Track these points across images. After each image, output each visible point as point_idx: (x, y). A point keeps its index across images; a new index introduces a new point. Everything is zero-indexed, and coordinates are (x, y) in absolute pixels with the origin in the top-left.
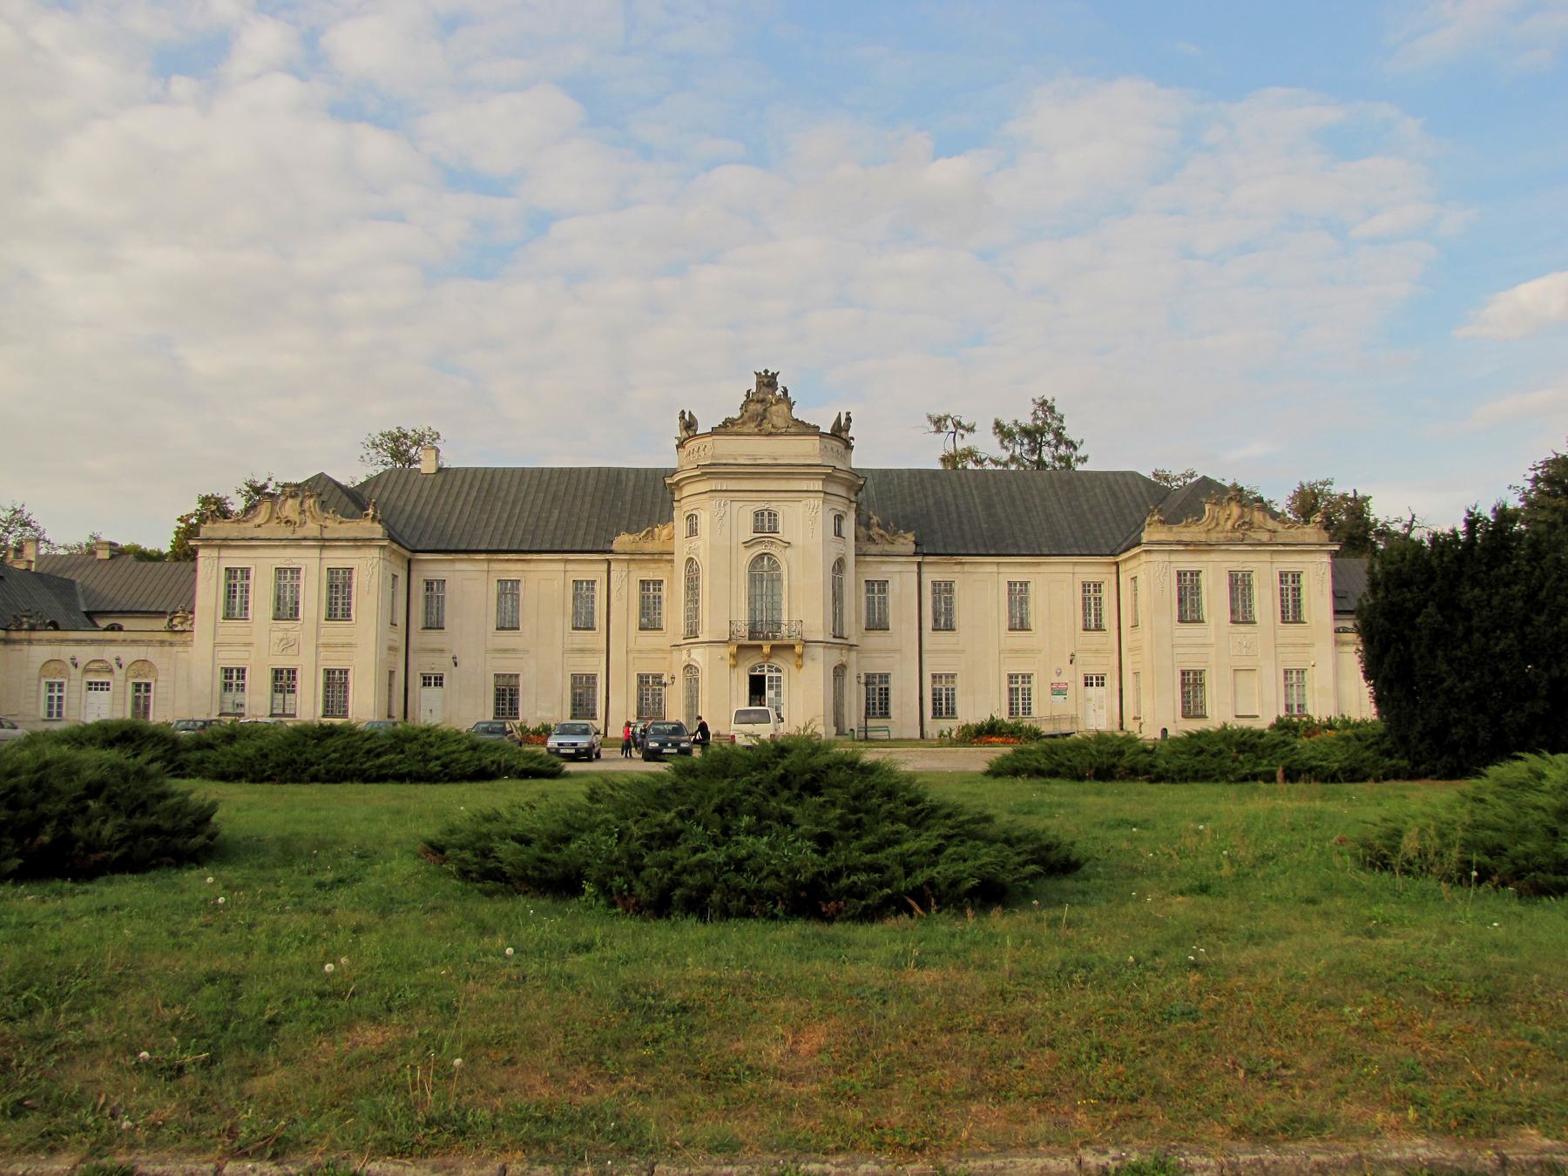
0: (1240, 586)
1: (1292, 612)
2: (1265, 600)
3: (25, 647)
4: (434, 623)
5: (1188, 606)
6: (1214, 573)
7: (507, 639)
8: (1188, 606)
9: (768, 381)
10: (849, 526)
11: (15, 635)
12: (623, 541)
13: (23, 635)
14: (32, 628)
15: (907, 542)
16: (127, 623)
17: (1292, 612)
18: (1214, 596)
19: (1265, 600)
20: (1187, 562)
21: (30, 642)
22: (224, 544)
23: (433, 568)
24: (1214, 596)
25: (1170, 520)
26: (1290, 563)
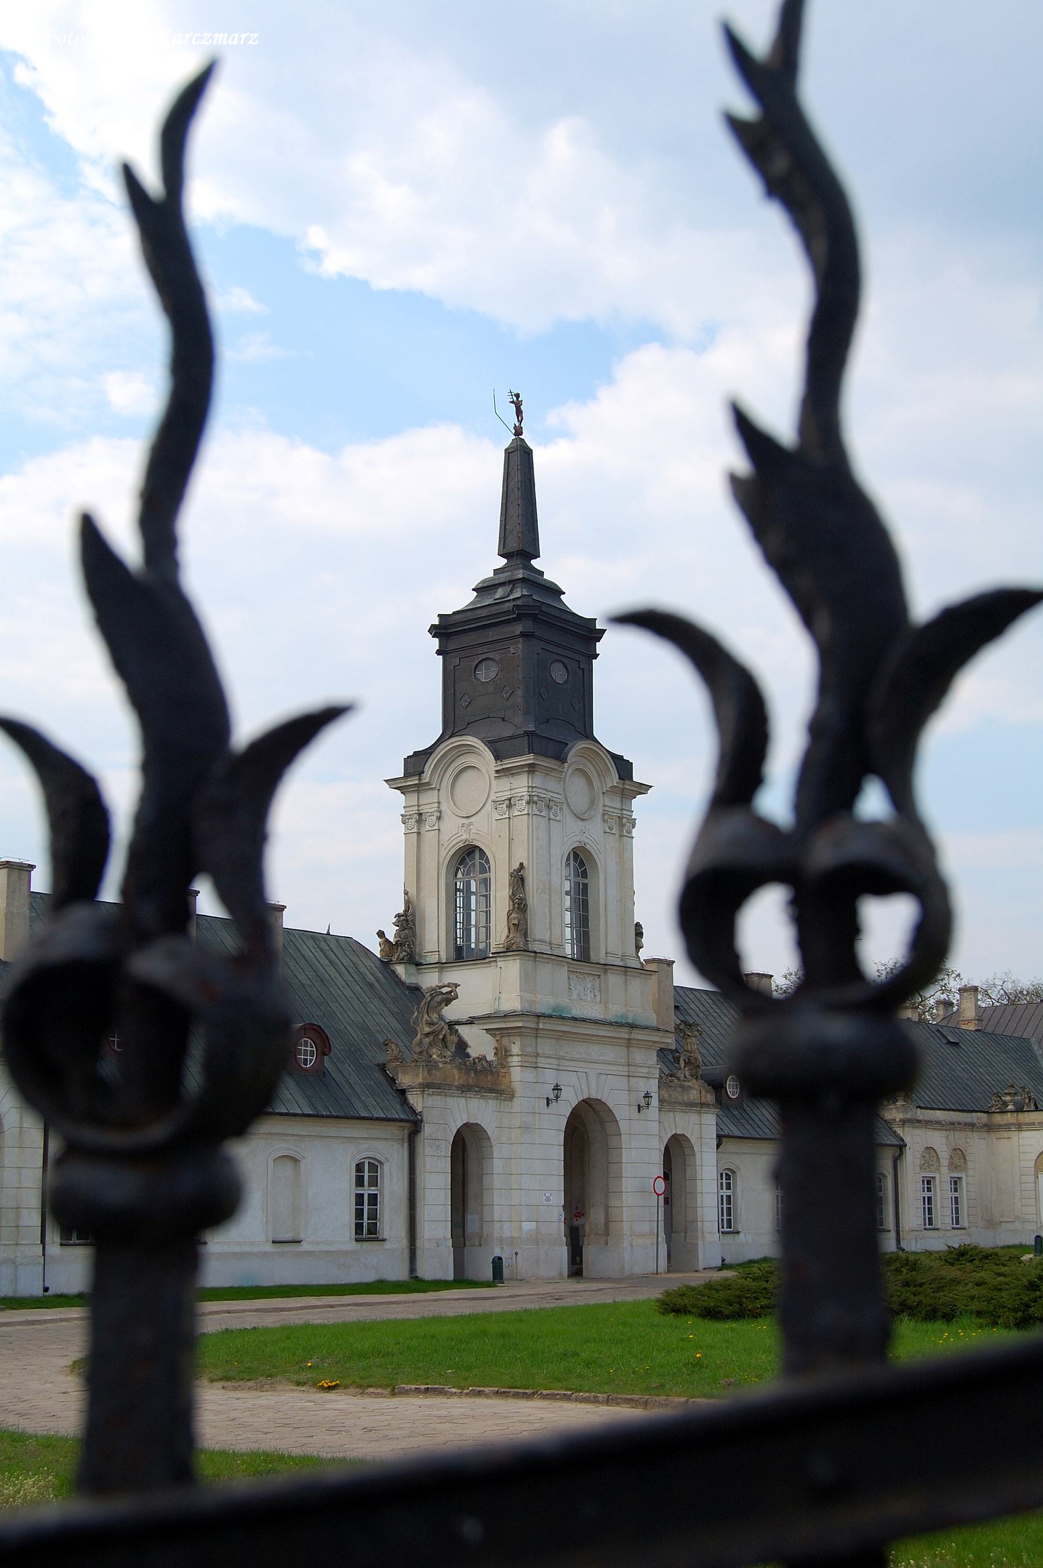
3: (1014, 1135)
11: (998, 1119)
13: (1009, 1118)
14: (1019, 1110)
21: (1019, 1127)
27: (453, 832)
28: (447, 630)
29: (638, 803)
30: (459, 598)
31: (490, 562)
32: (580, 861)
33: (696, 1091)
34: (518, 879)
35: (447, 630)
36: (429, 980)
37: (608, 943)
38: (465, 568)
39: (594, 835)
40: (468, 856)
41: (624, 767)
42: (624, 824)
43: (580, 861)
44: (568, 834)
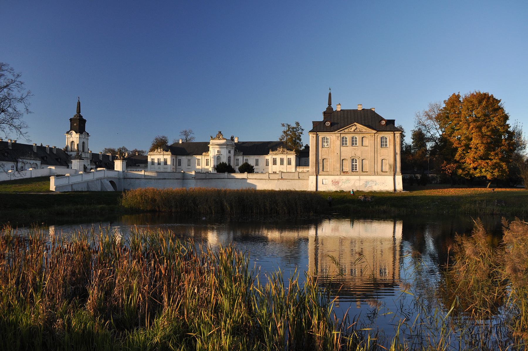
0: (282, 161)
1: (289, 163)
2: (285, 162)
4: (180, 165)
5: (275, 162)
6: (278, 157)
7: (189, 167)
8: (275, 162)
9: (220, 132)
10: (232, 152)
12: (204, 154)
15: (242, 153)
16: (141, 165)
17: (289, 163)
18: (278, 161)
19: (285, 162)
20: (274, 157)
22: (151, 155)
23: (180, 157)
24: (278, 161)
25: (272, 151)
26: (289, 157)
27: (71, 140)
28: (71, 120)
29: (89, 137)
30: (72, 117)
31: (75, 113)
32: (83, 143)
33: (94, 164)
34: (78, 145)
35: (71, 120)
36: (69, 153)
37: (86, 150)
38: (73, 114)
39: (85, 141)
40: (73, 142)
41: (88, 134)
42: (88, 139)
43: (83, 143)
44: (82, 140)
